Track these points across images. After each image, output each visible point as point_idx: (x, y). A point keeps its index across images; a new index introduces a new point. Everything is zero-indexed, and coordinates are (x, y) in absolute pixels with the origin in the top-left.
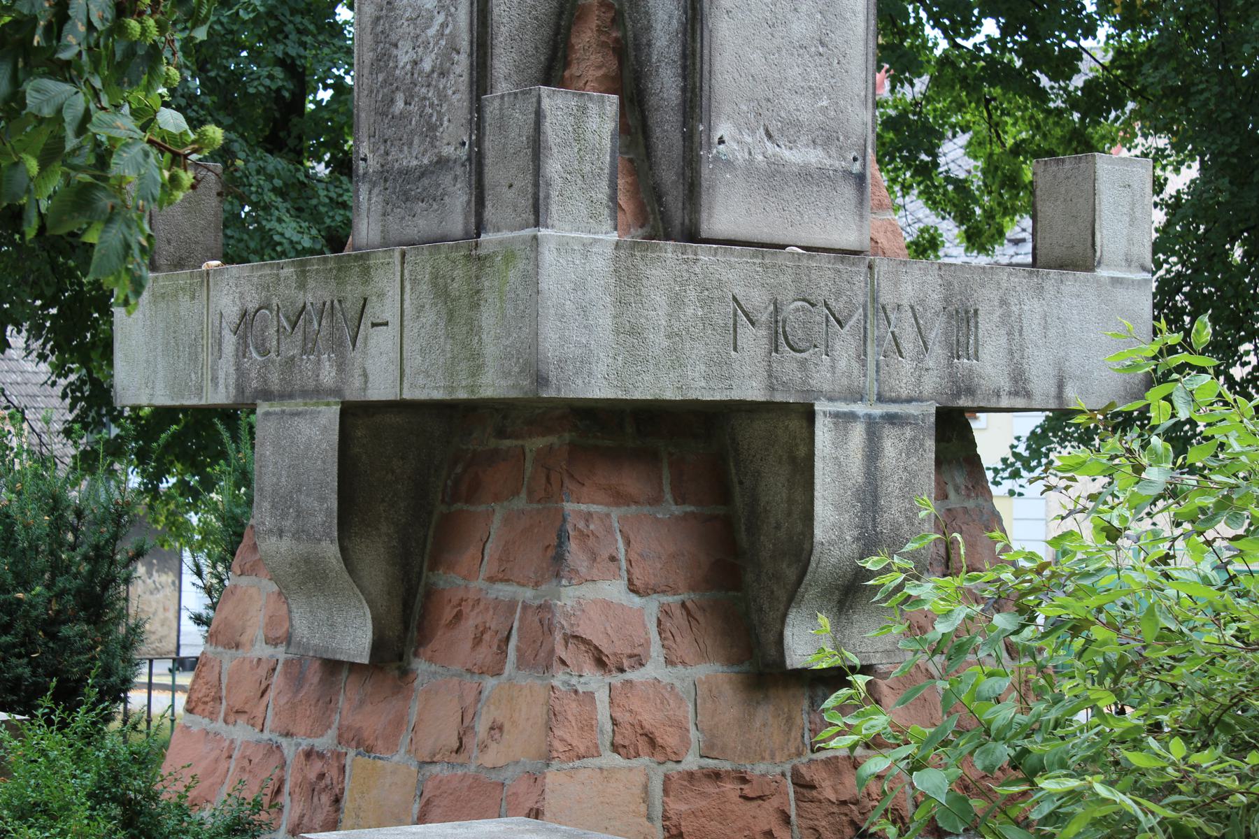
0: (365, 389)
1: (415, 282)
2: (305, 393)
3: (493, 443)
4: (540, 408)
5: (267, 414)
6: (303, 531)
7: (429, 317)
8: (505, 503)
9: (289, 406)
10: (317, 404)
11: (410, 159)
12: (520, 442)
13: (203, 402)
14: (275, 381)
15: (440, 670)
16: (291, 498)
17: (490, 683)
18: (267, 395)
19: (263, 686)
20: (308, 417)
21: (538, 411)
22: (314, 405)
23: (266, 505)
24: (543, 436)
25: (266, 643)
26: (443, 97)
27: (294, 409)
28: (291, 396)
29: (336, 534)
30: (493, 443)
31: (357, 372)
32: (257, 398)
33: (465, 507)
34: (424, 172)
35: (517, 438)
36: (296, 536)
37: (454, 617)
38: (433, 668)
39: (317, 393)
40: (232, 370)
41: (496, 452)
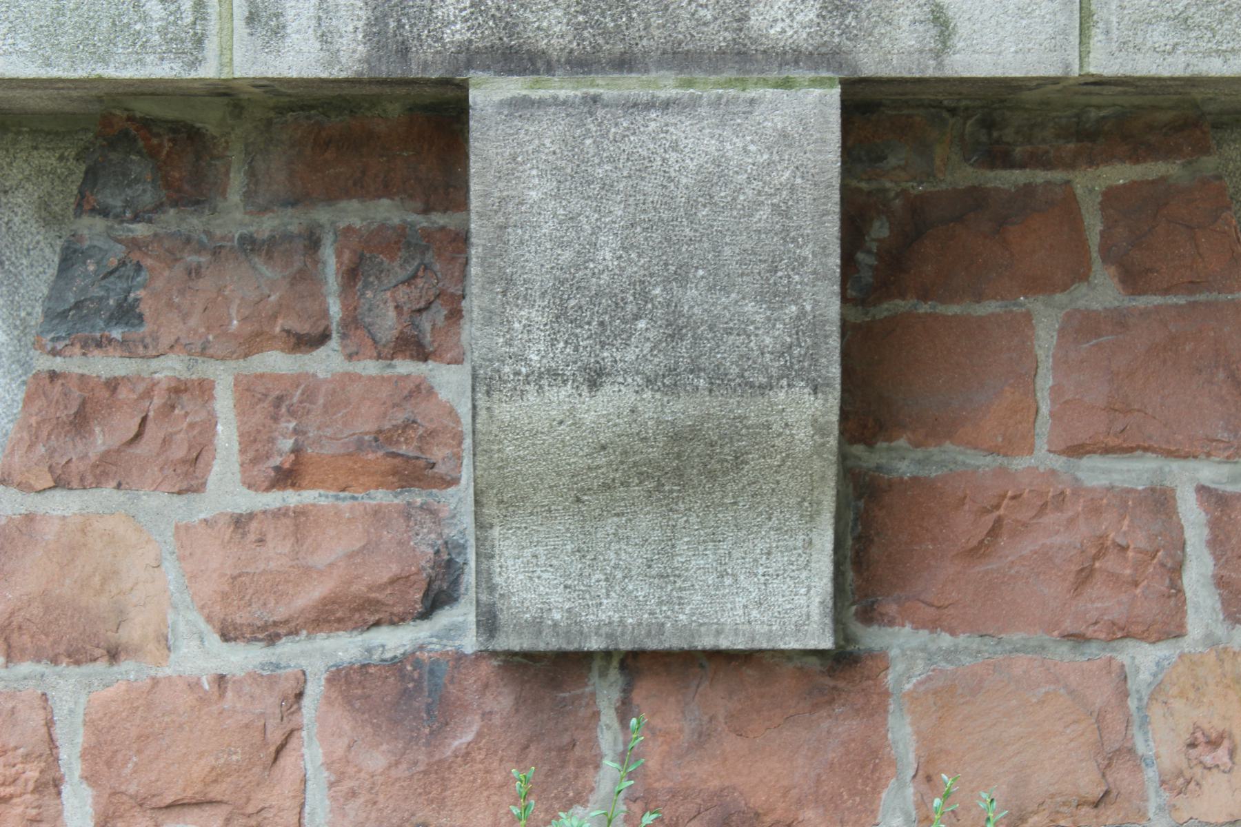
0: (938, 55)
3: (966, 175)
4: (1099, 107)
5: (519, 105)
6: (695, 370)
8: (1060, 297)
9: (631, 86)
10: (742, 83)
12: (1057, 175)
13: (208, 71)
15: (975, 643)
16: (645, 296)
19: (275, 737)
20: (703, 111)
21: (1093, 114)
22: (729, 84)
24: (1137, 162)
25: (225, 637)
27: (643, 94)
28: (624, 63)
29: (835, 371)
30: (966, 175)
32: (469, 65)
33: (924, 308)
35: (1047, 165)
37: (988, 534)
38: (946, 640)
41: (976, 198)
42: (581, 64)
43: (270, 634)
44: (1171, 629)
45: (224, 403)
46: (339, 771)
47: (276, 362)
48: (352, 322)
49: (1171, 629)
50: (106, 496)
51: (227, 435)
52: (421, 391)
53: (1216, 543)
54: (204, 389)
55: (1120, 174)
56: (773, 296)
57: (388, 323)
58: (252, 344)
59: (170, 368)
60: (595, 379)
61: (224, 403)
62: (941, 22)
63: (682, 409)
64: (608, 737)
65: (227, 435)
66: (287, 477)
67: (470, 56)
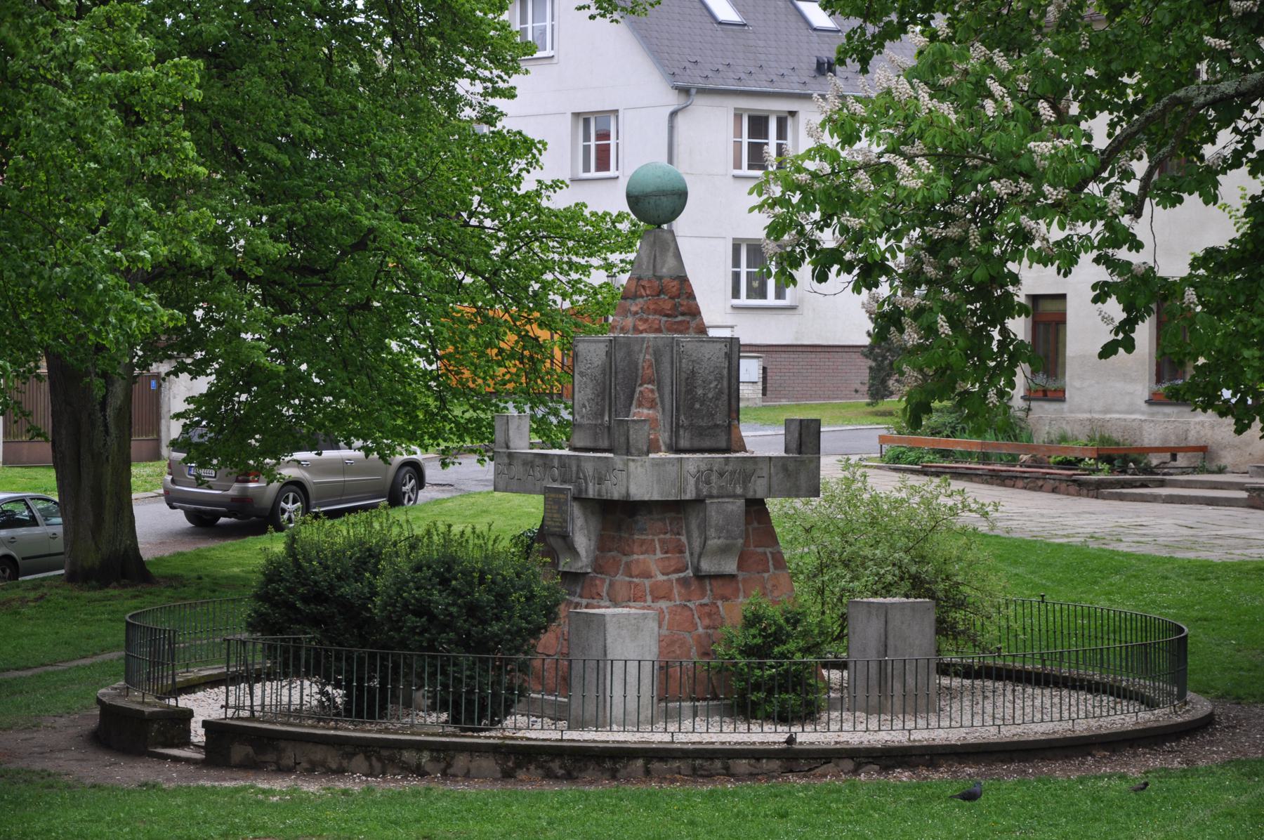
1: (775, 466)
2: (729, 496)
7: (781, 476)
9: (724, 500)
11: (703, 423)
14: (715, 492)
17: (766, 575)
18: (711, 497)
23: (712, 530)
26: (717, 406)
28: (722, 497)
31: (751, 490)
34: (709, 428)
36: (726, 538)
39: (735, 496)
40: (694, 489)
42: (718, 497)
43: (667, 574)
44: (768, 571)
45: (657, 542)
46: (679, 592)
47: (662, 536)
48: (671, 530)
49: (768, 571)
50: (646, 556)
51: (657, 546)
52: (680, 540)
53: (773, 558)
54: (653, 540)
55: (756, 508)
56: (738, 527)
57: (675, 530)
58: (659, 533)
59: (650, 537)
60: (719, 538)
61: (657, 542)
62: (755, 491)
63: (728, 542)
64: (708, 588)
65: (657, 546)
66: (666, 553)
67: (706, 496)
